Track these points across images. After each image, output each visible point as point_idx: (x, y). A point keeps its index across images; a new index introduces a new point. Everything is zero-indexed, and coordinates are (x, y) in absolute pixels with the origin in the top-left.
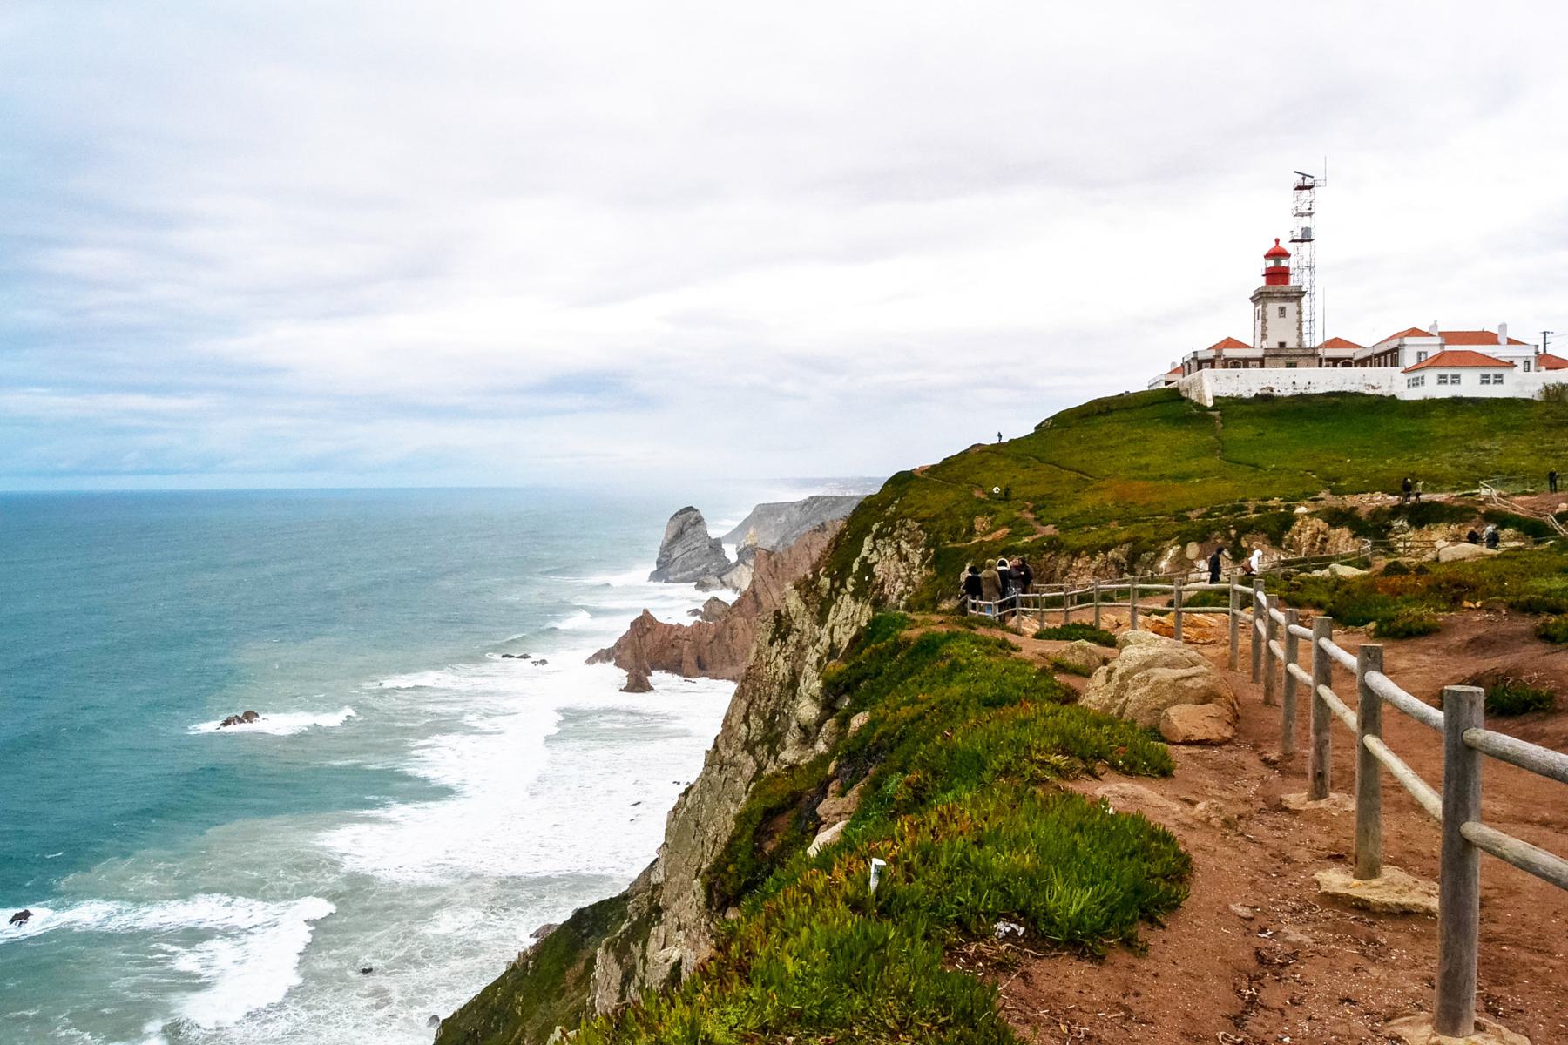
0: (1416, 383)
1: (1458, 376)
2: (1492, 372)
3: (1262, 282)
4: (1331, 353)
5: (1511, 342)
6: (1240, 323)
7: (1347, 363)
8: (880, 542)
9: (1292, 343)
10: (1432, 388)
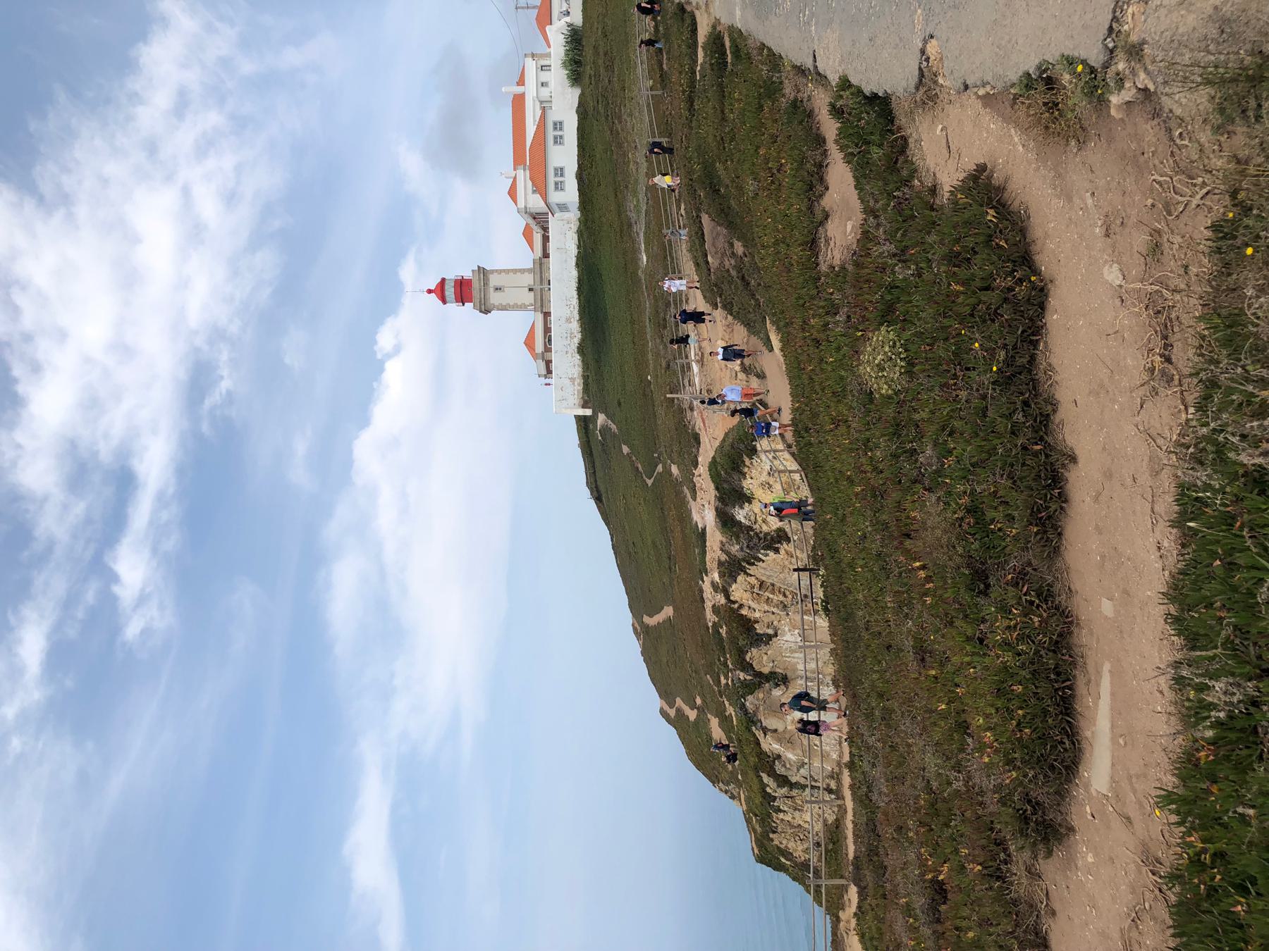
1: (556, 169)
2: (551, 134)
9: (529, 279)
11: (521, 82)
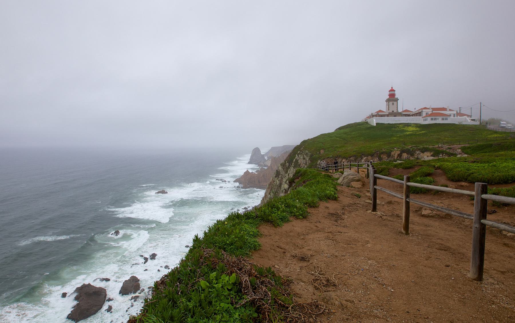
0: (426, 120)
2: (444, 117)
3: (388, 97)
4: (404, 113)
5: (450, 110)
6: (383, 107)
7: (409, 115)
10: (429, 121)
11: (450, 110)
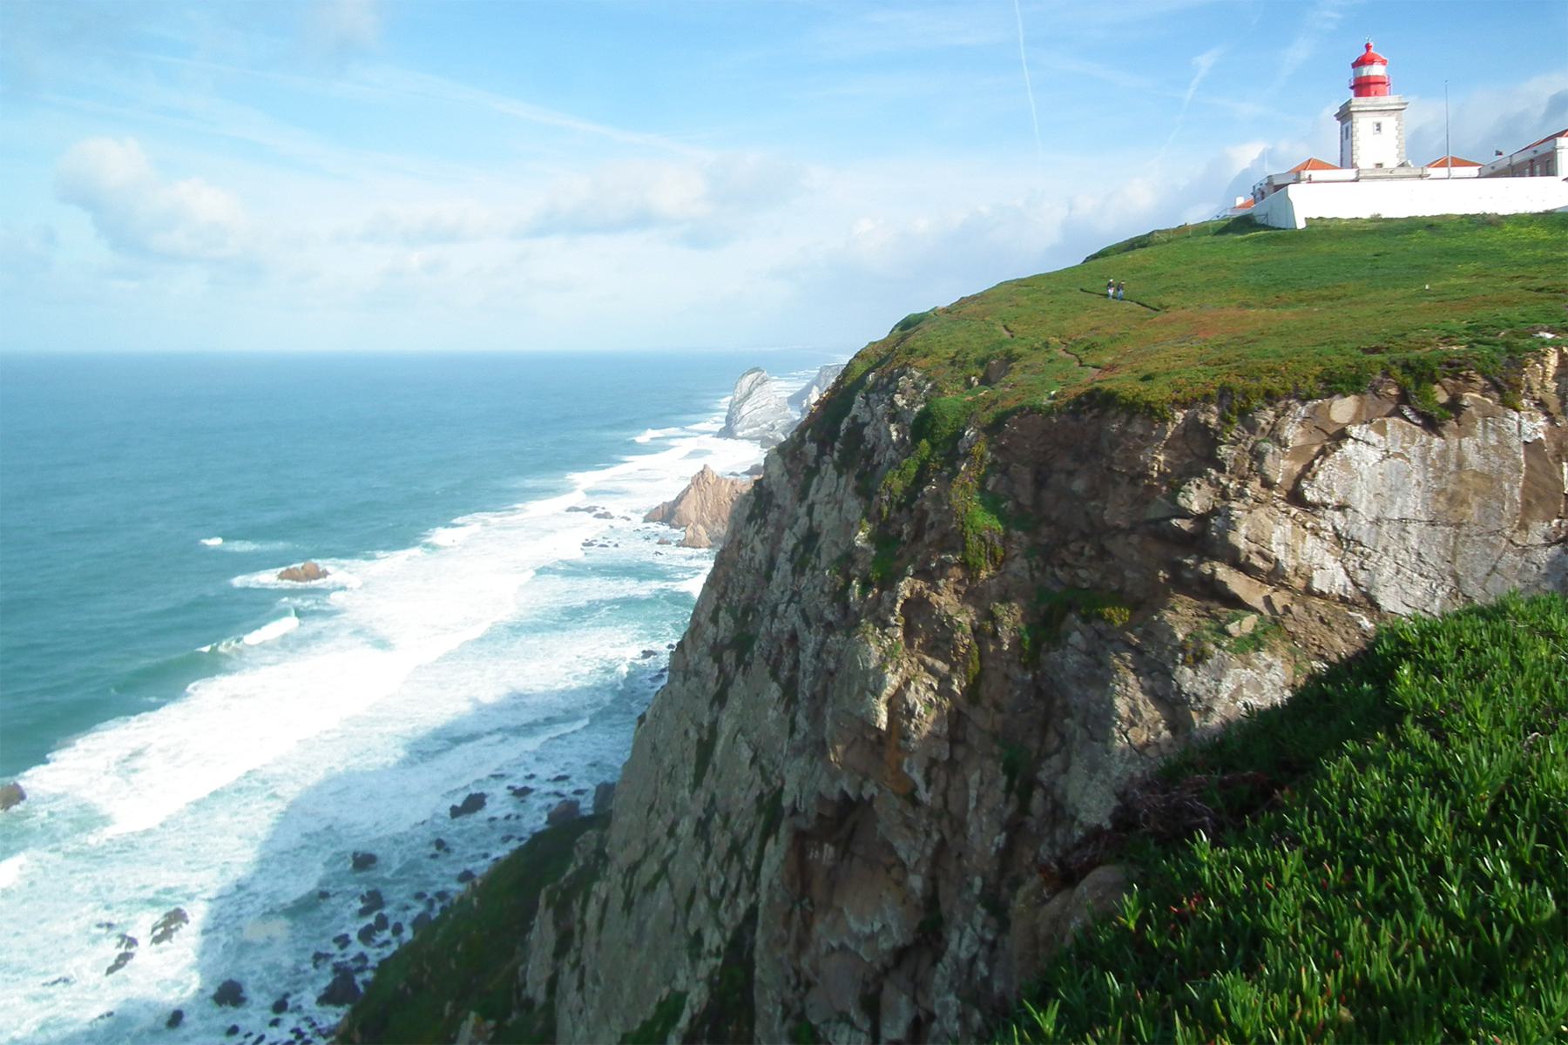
8: (873, 396)
9: (1391, 162)
